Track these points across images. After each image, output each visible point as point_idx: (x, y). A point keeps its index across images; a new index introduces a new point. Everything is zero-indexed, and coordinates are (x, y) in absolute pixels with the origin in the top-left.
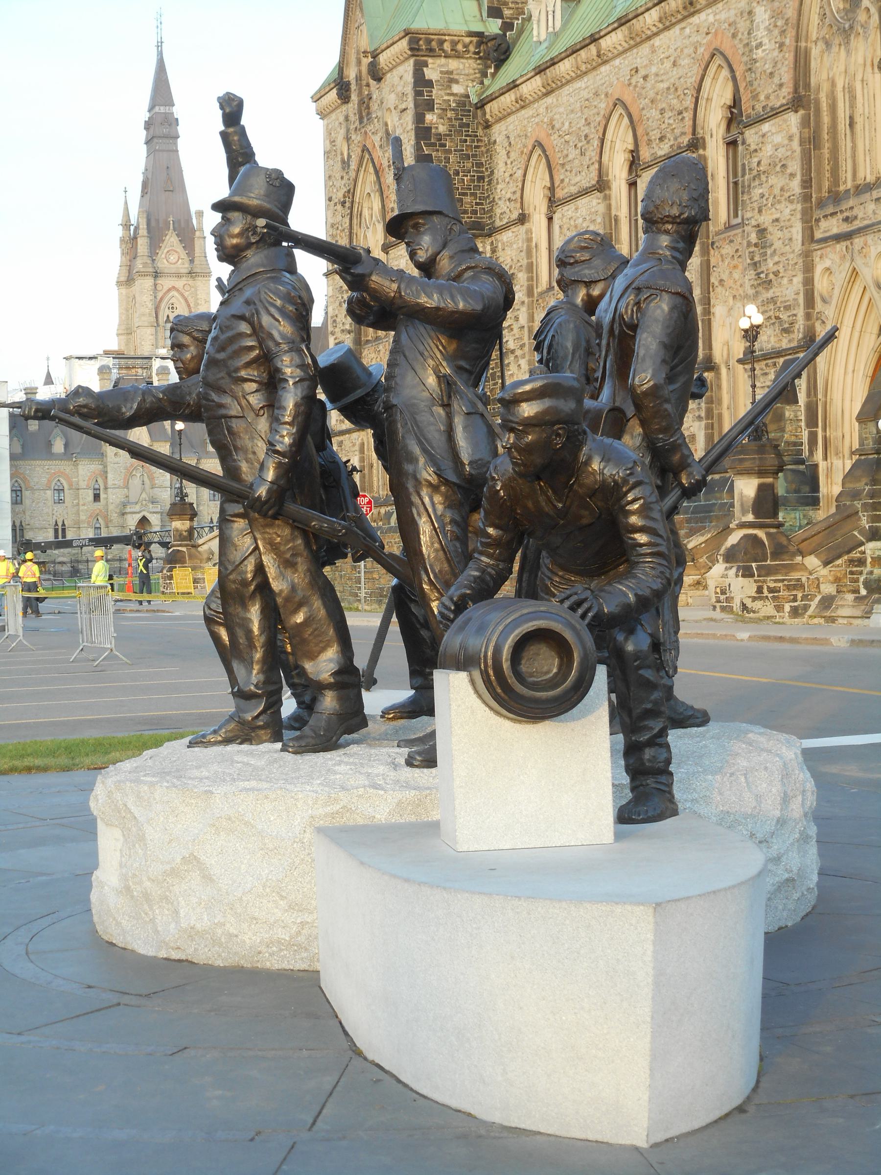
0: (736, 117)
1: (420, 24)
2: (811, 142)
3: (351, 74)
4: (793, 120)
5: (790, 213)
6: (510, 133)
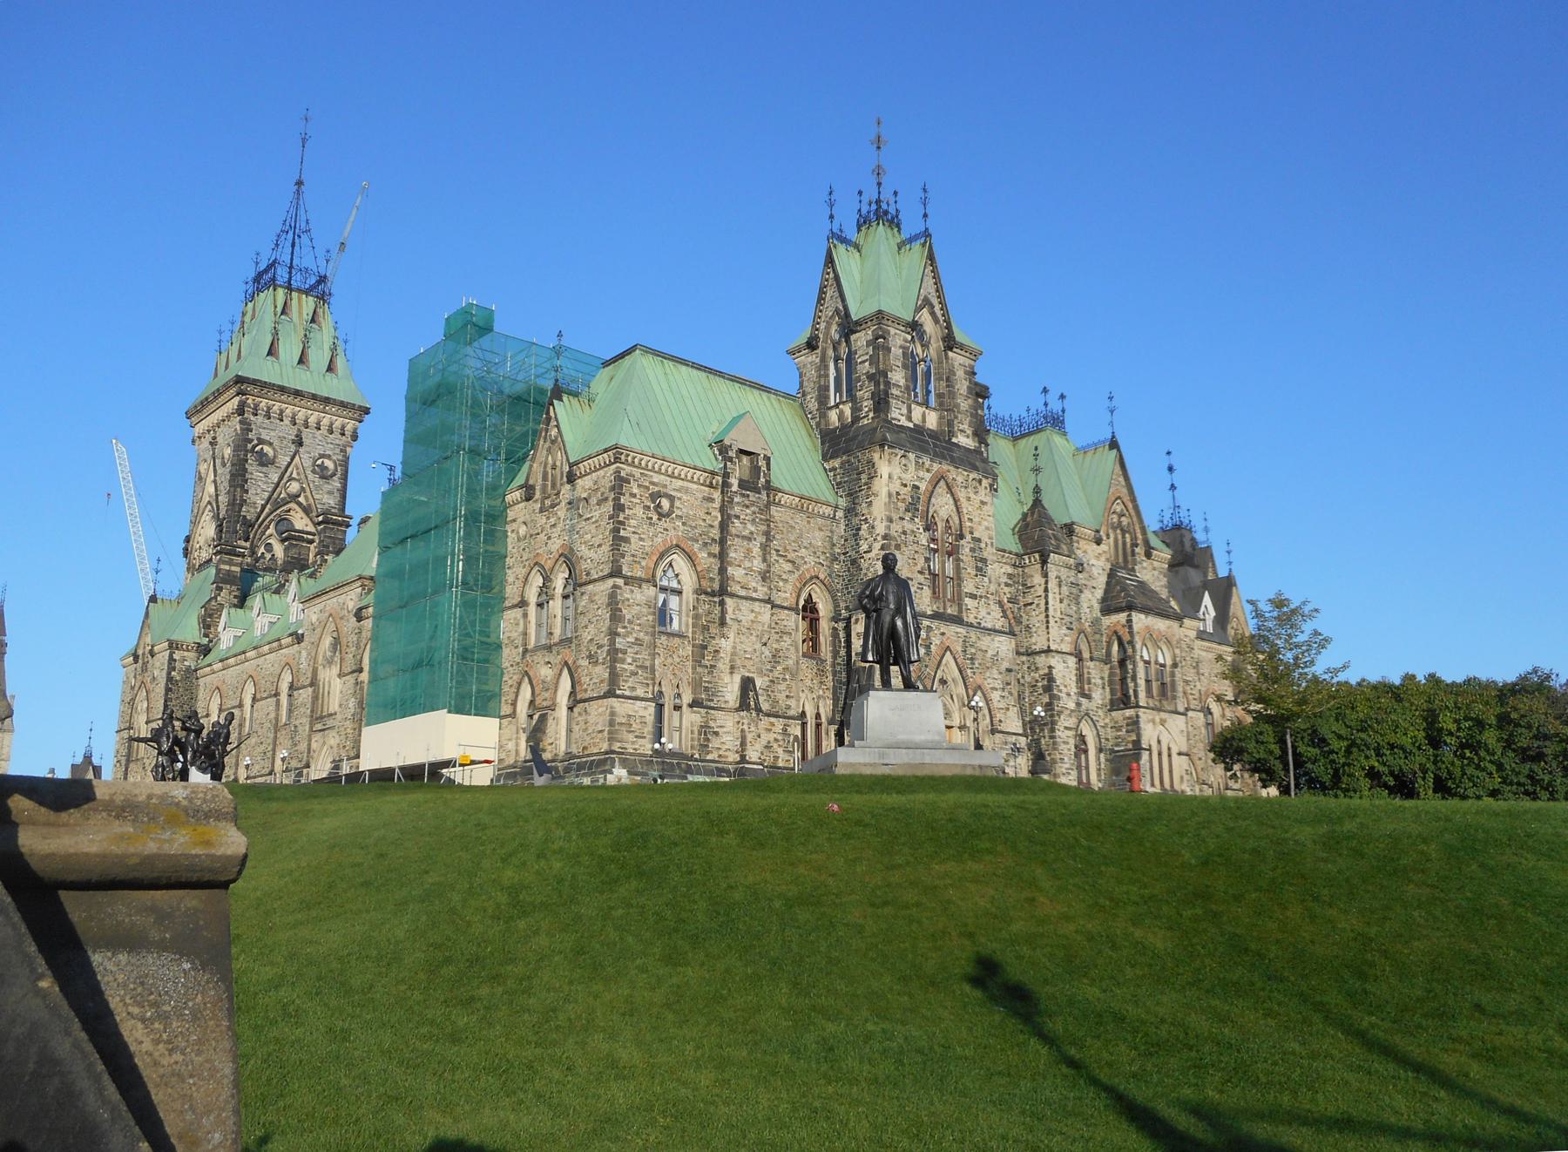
0: (292, 687)
1: (174, 637)
2: (315, 698)
3: (140, 652)
4: (310, 690)
5: (306, 721)
6: (205, 682)
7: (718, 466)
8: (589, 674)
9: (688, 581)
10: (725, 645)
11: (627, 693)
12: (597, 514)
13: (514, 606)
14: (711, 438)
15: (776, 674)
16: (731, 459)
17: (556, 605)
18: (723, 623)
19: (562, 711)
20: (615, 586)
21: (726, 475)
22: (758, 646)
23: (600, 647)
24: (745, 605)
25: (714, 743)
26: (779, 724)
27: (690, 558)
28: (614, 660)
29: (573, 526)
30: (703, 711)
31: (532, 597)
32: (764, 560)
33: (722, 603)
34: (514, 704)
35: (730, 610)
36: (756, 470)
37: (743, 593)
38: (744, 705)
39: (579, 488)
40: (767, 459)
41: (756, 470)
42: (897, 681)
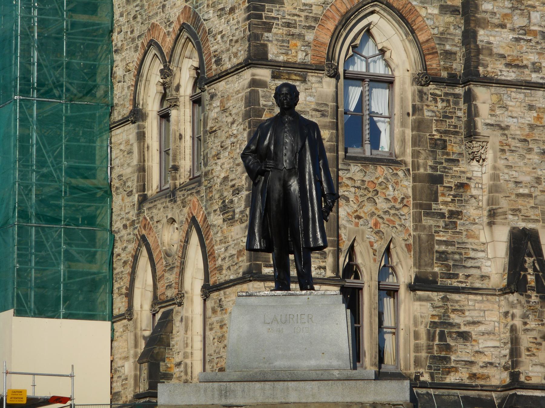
8: (224, 240)
9: (403, 60)
10: (479, 173)
13: (124, 121)
17: (183, 117)
18: (471, 133)
19: (194, 307)
20: (255, 83)
23: (237, 191)
24: (515, 98)
25: (461, 352)
27: (405, 19)
30: (436, 296)
31: (152, 106)
33: (469, 97)
34: (130, 295)
35: (484, 109)
37: (511, 75)
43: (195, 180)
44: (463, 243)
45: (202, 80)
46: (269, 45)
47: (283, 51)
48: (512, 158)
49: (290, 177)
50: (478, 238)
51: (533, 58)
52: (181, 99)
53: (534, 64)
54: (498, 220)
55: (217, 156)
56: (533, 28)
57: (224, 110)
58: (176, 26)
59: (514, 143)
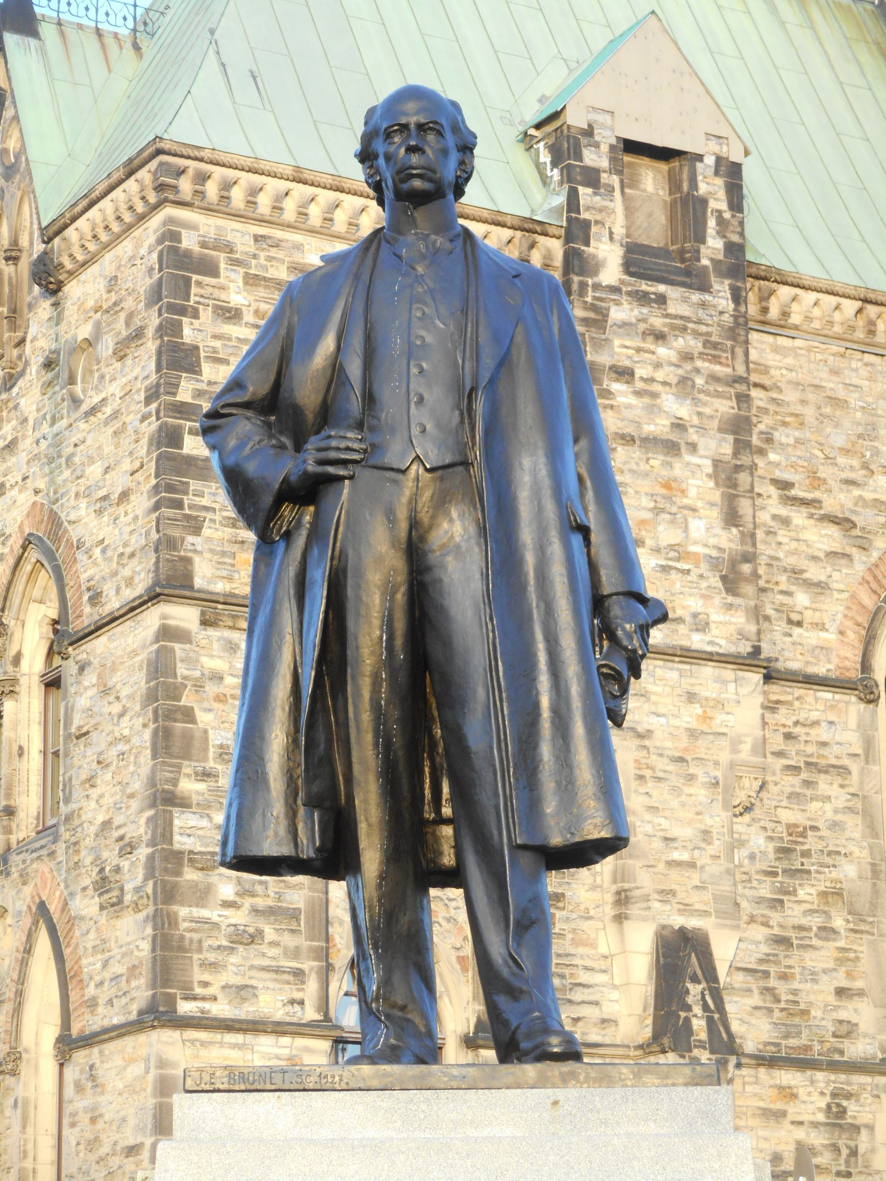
7: (546, 202)
8: (102, 947)
11: (221, 1009)
12: (114, 389)
14: (533, 113)
15: (794, 914)
16: (592, 178)
20: (166, 633)
21: (577, 231)
22: (717, 819)
23: (128, 848)
26: (812, 1093)
28: (168, 894)
29: (58, 441)
32: (732, 518)
36: (688, 210)
38: (668, 1029)
39: (70, 310)
40: (732, 174)
41: (688, 210)
42: (458, 1004)
43: (47, 831)
44: (567, 955)
45: (64, 637)
46: (197, 560)
47: (224, 573)
48: (659, 793)
49: (441, 502)
50: (594, 945)
51: (694, 604)
52: (24, 681)
53: (695, 615)
54: (634, 910)
55: (91, 781)
56: (693, 549)
57: (105, 691)
58: (16, 542)
59: (662, 764)
